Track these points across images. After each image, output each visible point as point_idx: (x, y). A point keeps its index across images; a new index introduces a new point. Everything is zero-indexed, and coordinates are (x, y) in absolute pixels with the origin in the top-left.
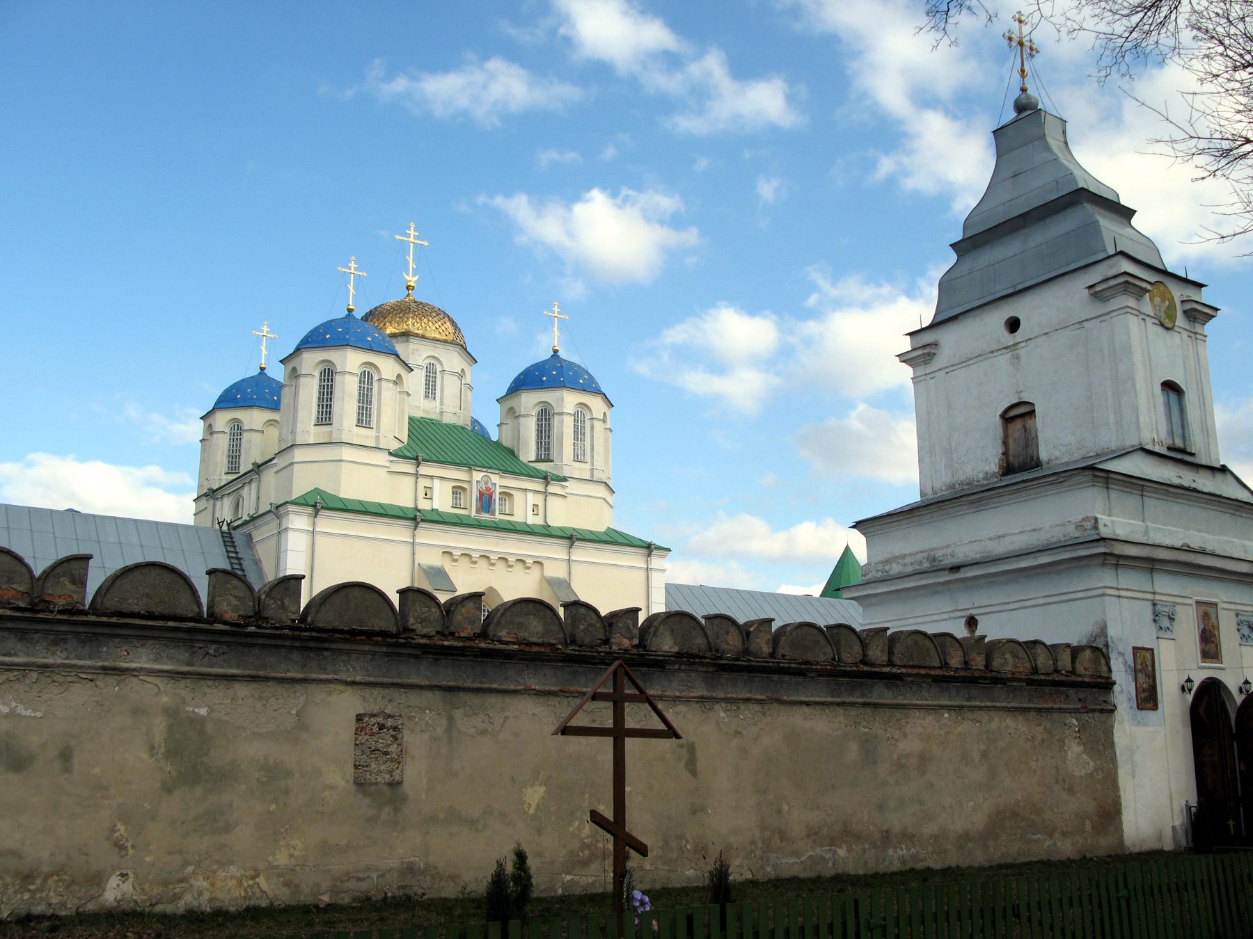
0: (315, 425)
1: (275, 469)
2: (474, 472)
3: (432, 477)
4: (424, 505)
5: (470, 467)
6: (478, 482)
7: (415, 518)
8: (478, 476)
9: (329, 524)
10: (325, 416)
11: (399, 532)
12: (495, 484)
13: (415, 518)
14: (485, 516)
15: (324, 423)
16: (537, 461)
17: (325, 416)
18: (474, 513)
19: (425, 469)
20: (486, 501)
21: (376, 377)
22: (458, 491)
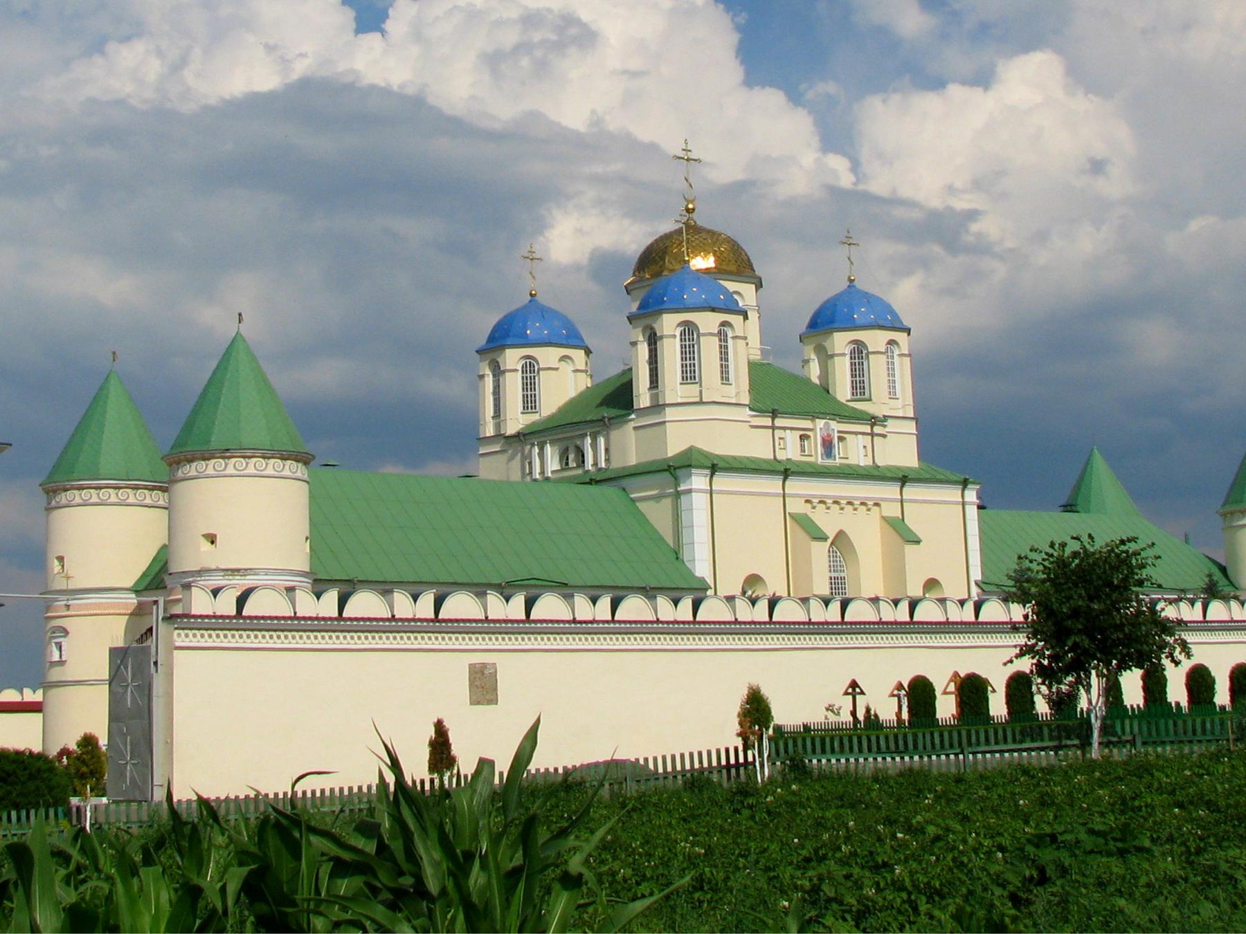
0: (681, 384)
1: (632, 424)
2: (817, 420)
3: (784, 428)
4: (781, 456)
5: (813, 416)
6: (821, 429)
7: (786, 472)
8: (820, 423)
9: (723, 482)
10: (690, 374)
11: (773, 484)
12: (833, 430)
13: (786, 472)
14: (829, 462)
15: (689, 381)
16: (848, 401)
17: (690, 374)
18: (820, 460)
19: (779, 422)
20: (828, 445)
21: (730, 334)
22: (802, 438)
